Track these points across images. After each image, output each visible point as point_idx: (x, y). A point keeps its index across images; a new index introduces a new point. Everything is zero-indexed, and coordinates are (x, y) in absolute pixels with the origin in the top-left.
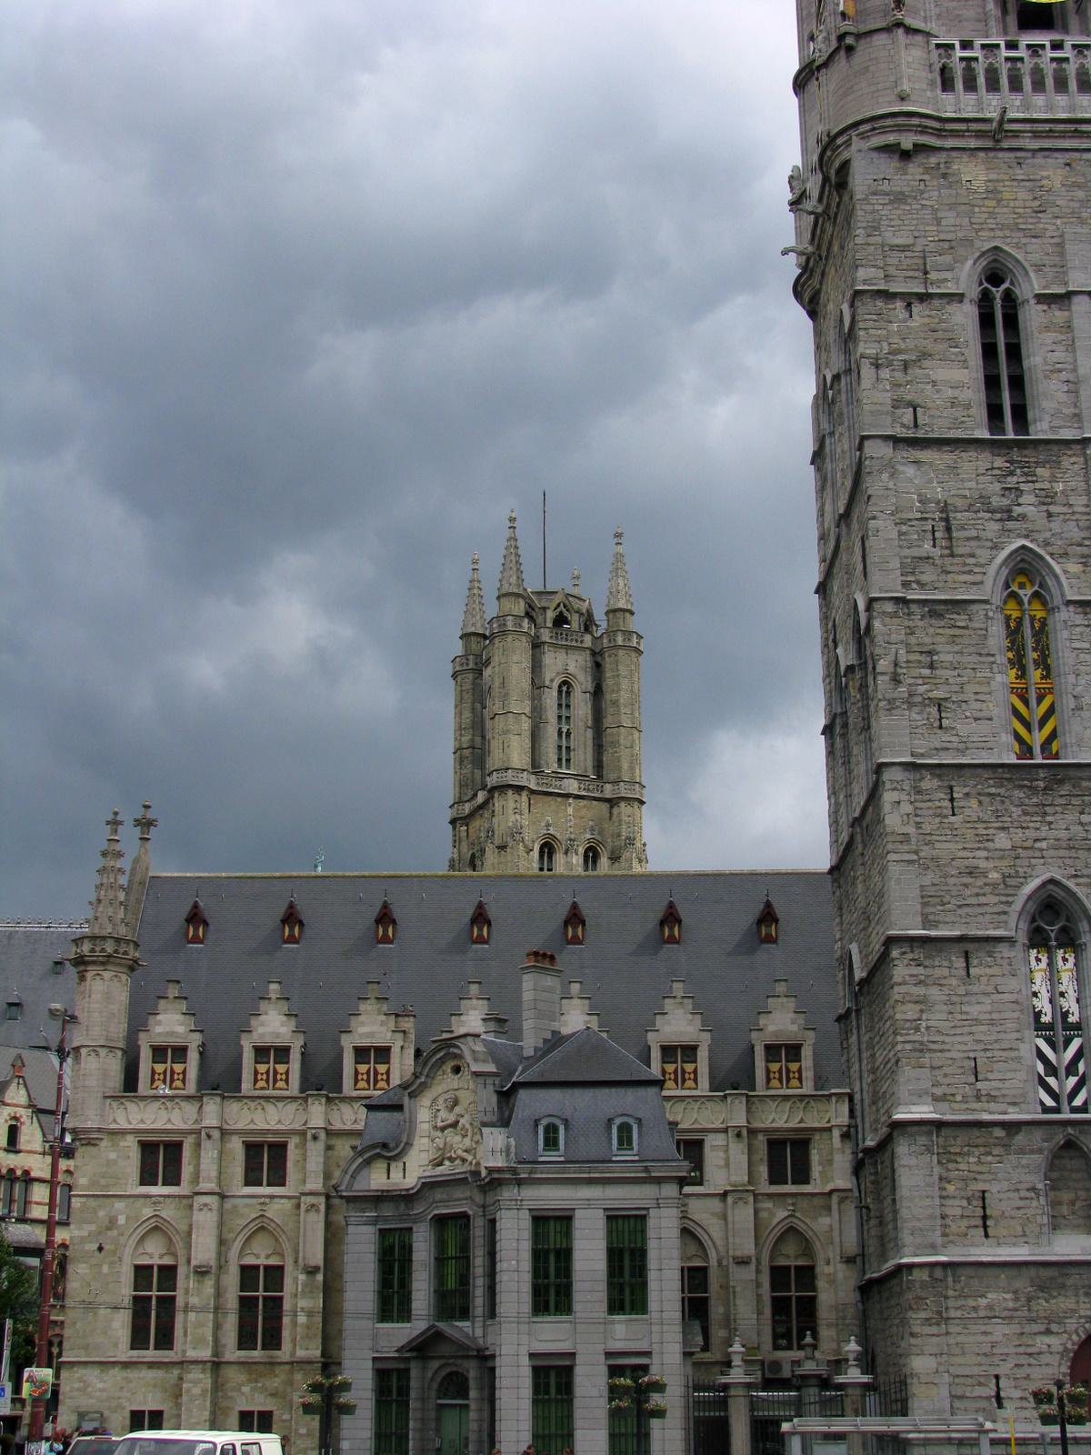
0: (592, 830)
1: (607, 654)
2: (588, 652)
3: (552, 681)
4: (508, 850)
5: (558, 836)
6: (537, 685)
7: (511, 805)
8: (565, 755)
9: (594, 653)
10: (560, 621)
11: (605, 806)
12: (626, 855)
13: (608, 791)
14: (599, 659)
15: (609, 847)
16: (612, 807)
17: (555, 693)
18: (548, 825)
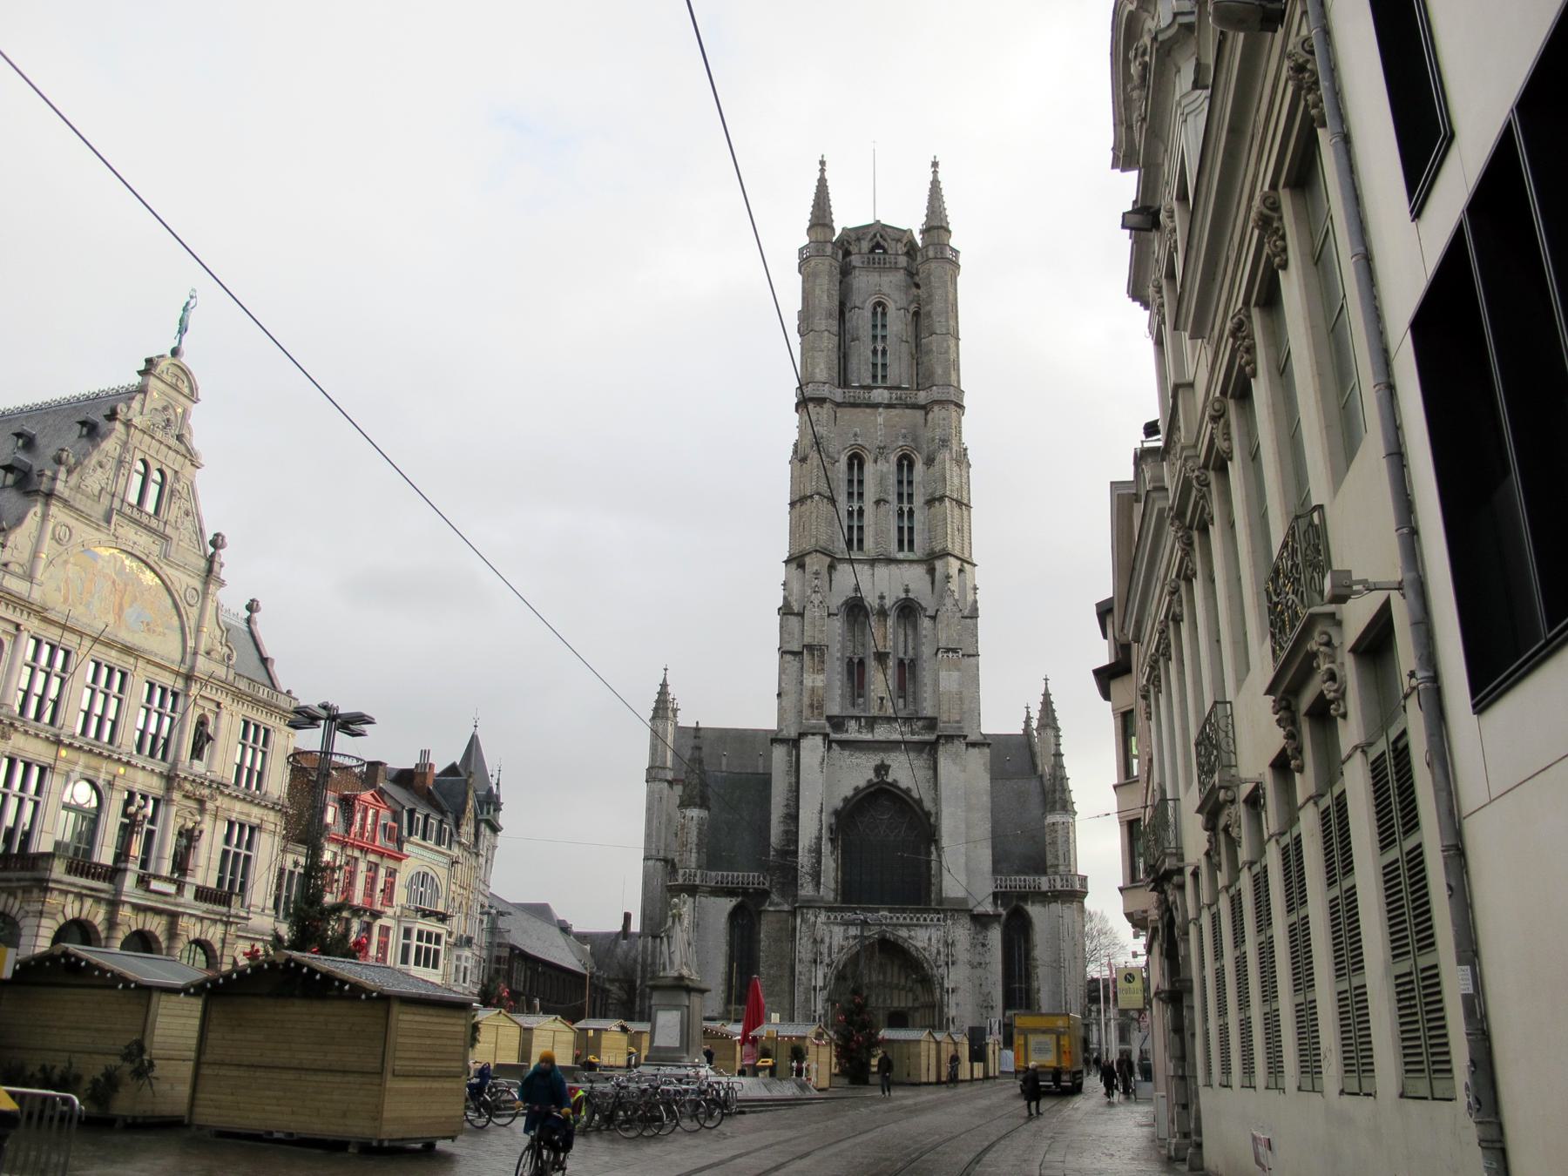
0: (905, 436)
2: (902, 271)
3: (864, 302)
4: (808, 462)
5: (867, 447)
11: (920, 414)
12: (939, 458)
13: (922, 397)
14: (917, 279)
15: (925, 453)
16: (927, 414)
17: (868, 314)
18: (855, 435)
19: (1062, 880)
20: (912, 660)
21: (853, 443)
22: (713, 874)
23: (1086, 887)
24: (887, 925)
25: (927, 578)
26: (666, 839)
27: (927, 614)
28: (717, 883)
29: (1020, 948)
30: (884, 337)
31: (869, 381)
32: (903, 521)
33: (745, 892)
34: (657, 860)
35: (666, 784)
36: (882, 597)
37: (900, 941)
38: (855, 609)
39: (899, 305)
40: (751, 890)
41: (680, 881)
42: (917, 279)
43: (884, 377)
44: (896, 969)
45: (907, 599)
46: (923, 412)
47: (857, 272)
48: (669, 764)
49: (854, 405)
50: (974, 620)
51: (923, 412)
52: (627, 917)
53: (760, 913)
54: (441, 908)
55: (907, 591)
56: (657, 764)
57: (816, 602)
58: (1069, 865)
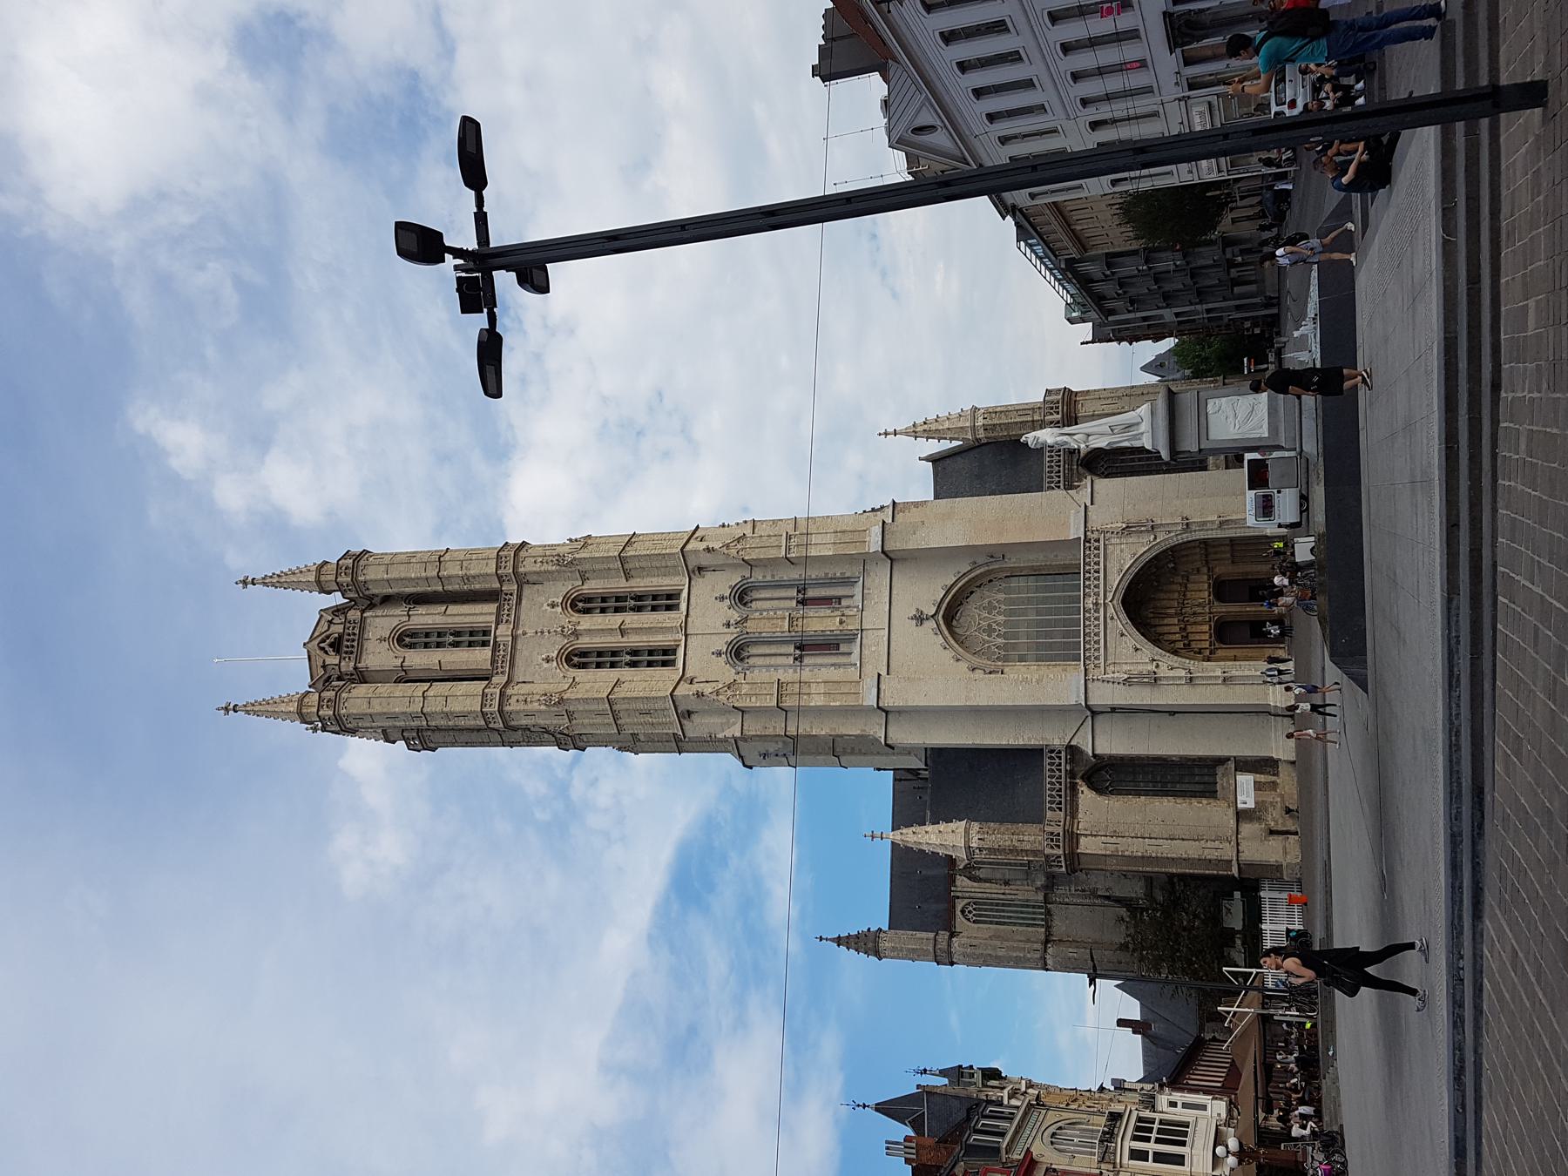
1: (367, 593)
2: (365, 615)
6: (405, 676)
7: (521, 707)
8: (476, 637)
9: (371, 606)
10: (337, 646)
11: (527, 590)
14: (377, 600)
18: (548, 660)
19: (1051, 414)
20: (799, 592)
21: (555, 663)
22: (1049, 813)
23: (1060, 390)
24: (1105, 598)
25: (708, 575)
26: (1021, 941)
27: (748, 575)
28: (1060, 809)
29: (1133, 460)
30: (439, 635)
31: (487, 652)
32: (646, 606)
33: (1072, 774)
34: (1045, 951)
35: (954, 939)
36: (728, 625)
37: (1125, 584)
38: (737, 652)
39: (407, 618)
40: (1068, 768)
41: (1060, 852)
42: (377, 600)
43: (486, 633)
44: (1162, 596)
45: (732, 596)
46: (526, 587)
47: (359, 665)
48: (931, 935)
49: (512, 665)
50: (758, 524)
51: (526, 587)
52: (1122, 1023)
53: (1095, 756)
54: (1103, 1120)
55: (722, 598)
56: (931, 948)
57: (729, 693)
58: (1033, 409)
